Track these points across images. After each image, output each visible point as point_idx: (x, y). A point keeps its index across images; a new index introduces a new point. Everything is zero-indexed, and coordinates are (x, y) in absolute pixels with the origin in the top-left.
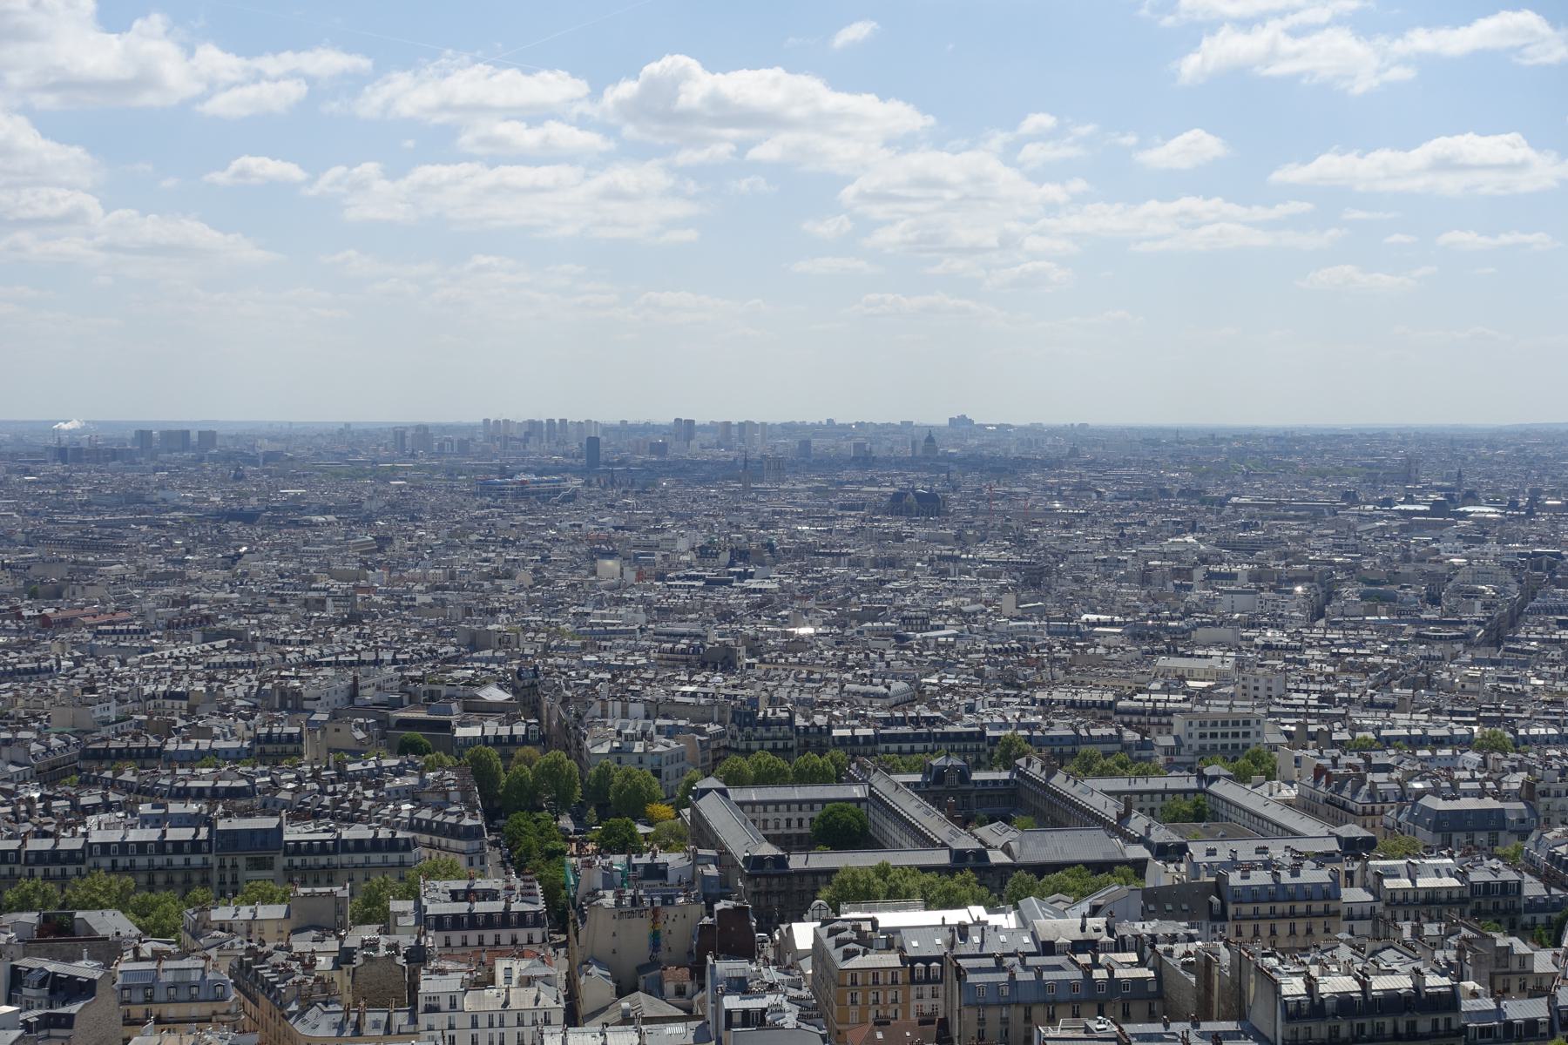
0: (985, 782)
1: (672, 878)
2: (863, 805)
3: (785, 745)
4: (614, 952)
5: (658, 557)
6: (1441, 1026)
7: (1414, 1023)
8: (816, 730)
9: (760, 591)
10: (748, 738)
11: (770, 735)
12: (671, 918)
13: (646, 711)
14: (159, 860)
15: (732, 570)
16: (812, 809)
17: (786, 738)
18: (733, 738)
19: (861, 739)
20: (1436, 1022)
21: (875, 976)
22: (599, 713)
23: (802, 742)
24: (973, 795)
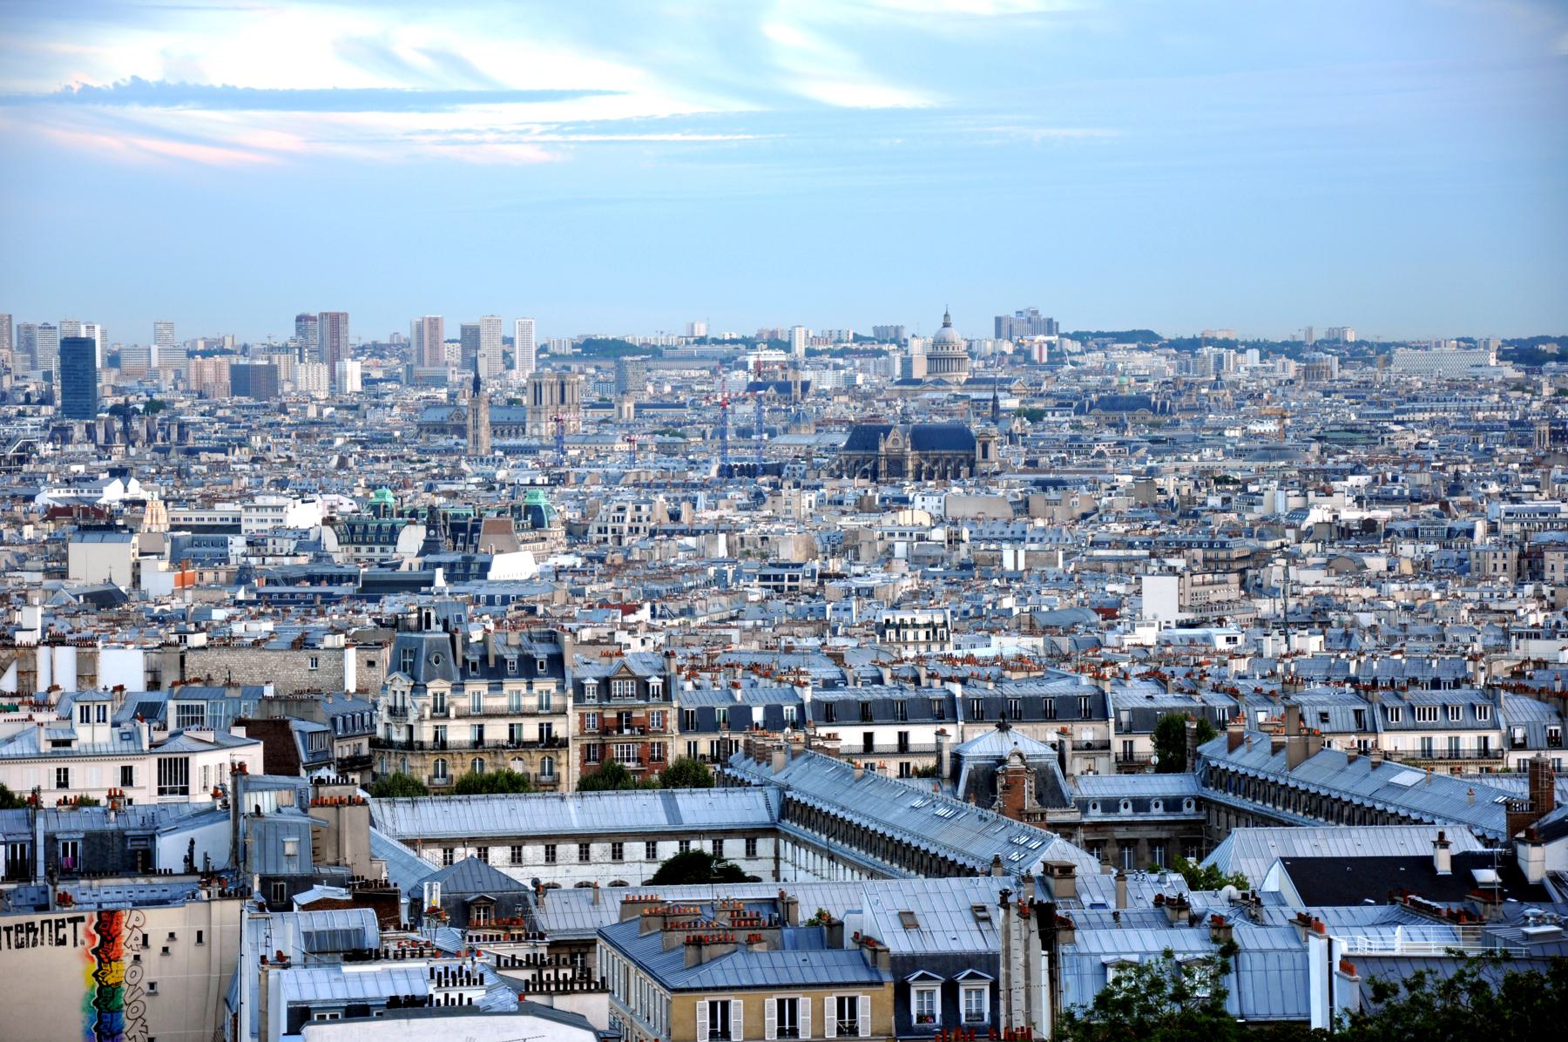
0: (1110, 805)
1: (170, 851)
2: (764, 846)
3: (545, 730)
8: (630, 687)
9: (506, 600)
10: (440, 711)
11: (499, 702)
12: (157, 942)
15: (430, 558)
16: (617, 855)
17: (547, 710)
19: (758, 715)
21: (787, 1012)
23: (593, 725)
24: (1081, 835)
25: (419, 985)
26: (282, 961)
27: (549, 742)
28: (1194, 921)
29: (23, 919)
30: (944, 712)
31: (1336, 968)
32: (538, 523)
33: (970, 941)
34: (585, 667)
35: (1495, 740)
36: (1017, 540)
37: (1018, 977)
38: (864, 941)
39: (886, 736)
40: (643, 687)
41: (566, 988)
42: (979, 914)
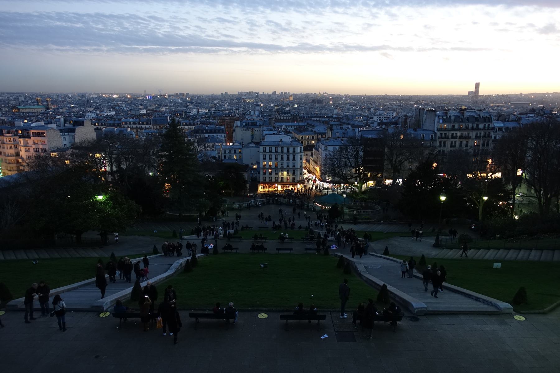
1: (258, 124)
4: (242, 139)
5: (268, 107)
6: (486, 126)
7: (478, 126)
10: (281, 116)
11: (285, 116)
12: (256, 131)
13: (259, 113)
14: (139, 126)
16: (294, 127)
17: (289, 117)
18: (277, 116)
19: (305, 117)
20: (485, 125)
22: (249, 114)
23: (293, 118)
25: (276, 133)
26: (264, 130)
27: (289, 119)
28: (344, 129)
29: (245, 128)
30: (320, 117)
31: (359, 131)
32: (289, 106)
33: (324, 131)
34: (292, 113)
35: (362, 120)
36: (325, 107)
37: (328, 135)
38: (314, 131)
39: (315, 119)
40: (296, 114)
41: (289, 133)
42: (325, 129)
